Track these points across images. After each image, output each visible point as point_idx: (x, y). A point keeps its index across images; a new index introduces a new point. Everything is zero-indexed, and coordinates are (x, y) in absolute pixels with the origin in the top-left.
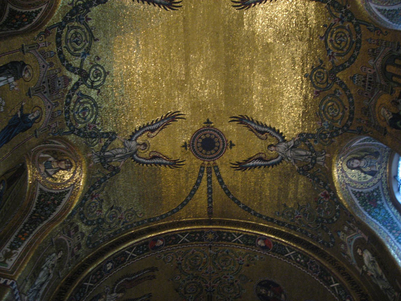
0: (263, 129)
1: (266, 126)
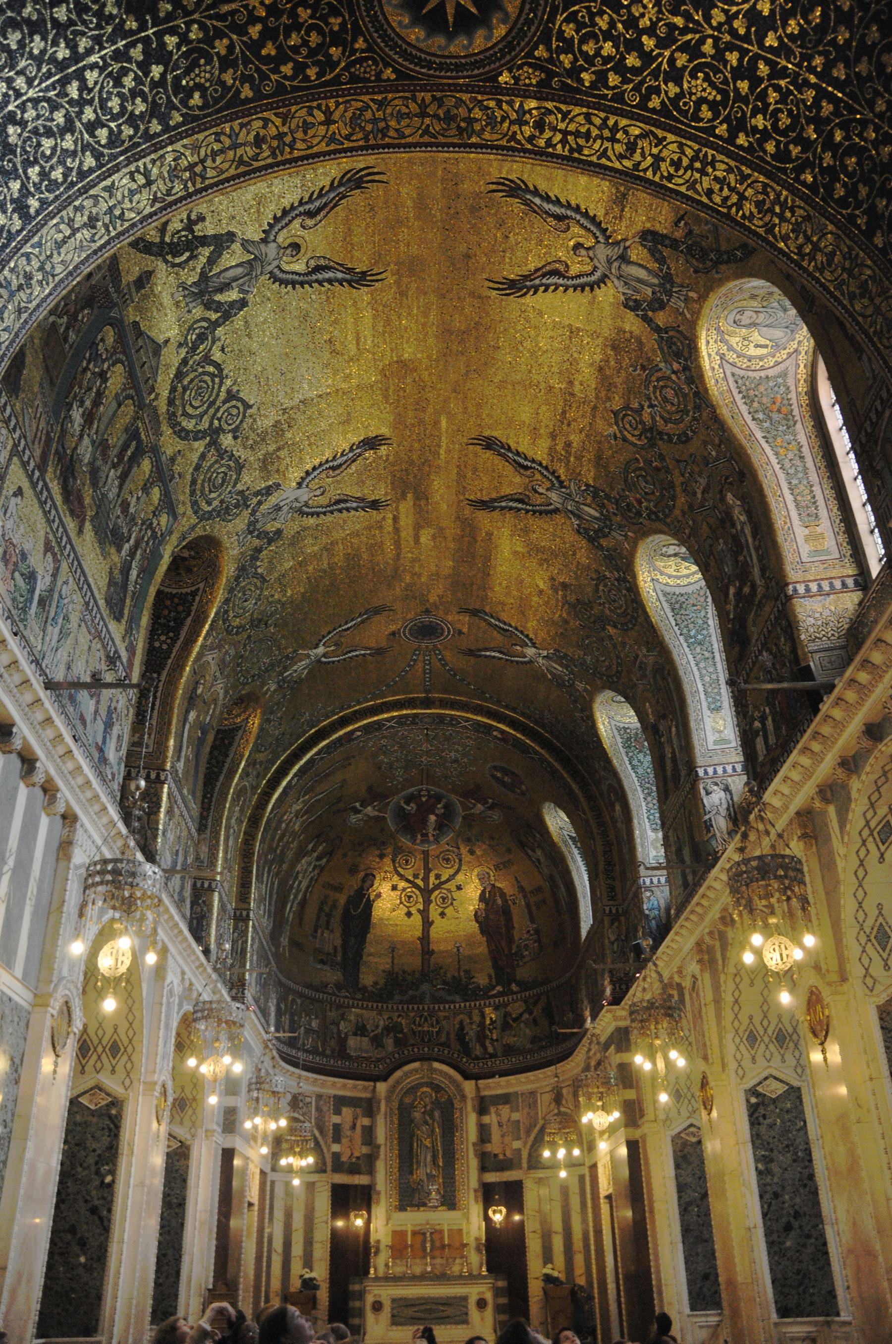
0: (507, 627)
1: (510, 626)
